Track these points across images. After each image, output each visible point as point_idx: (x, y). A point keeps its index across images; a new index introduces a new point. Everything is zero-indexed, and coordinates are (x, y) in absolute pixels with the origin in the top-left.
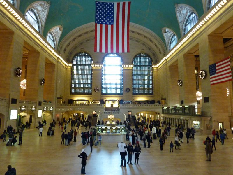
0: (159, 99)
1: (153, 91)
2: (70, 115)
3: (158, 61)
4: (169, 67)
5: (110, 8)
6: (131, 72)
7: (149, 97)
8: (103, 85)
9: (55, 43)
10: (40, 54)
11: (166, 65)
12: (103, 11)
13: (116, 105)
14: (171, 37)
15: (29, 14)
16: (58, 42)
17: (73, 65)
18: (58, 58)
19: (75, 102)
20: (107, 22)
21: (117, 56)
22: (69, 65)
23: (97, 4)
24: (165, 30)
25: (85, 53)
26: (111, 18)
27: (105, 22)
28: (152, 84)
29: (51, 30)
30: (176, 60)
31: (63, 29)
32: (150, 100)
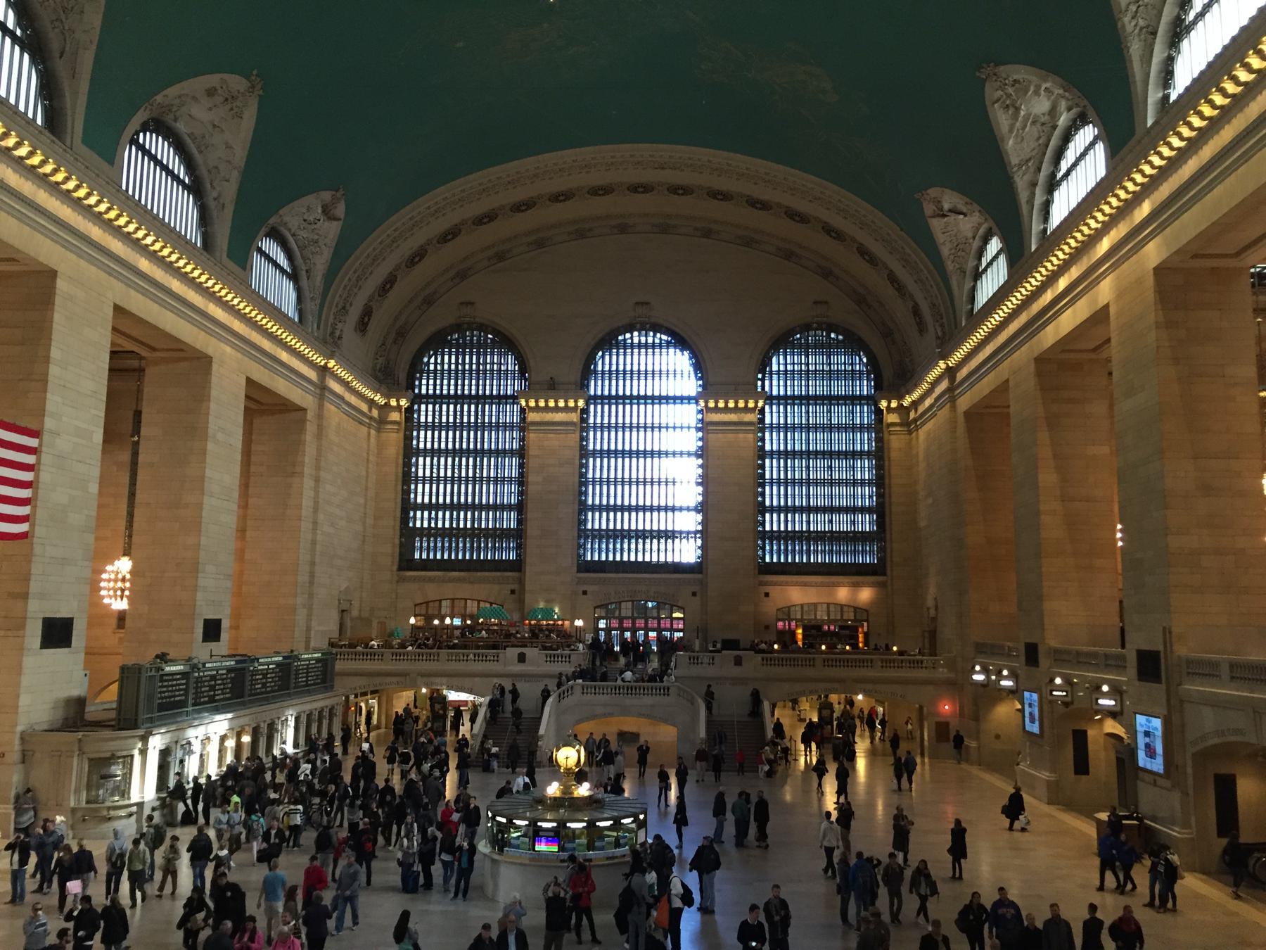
1: (882, 550)
4: (967, 414)
8: (590, 514)
9: (304, 282)
10: (215, 367)
11: (953, 400)
14: (976, 244)
15: (146, 152)
16: (318, 279)
17: (419, 399)
21: (668, 344)
24: (938, 202)
25: (483, 328)
28: (880, 511)
29: (272, 221)
30: (998, 382)
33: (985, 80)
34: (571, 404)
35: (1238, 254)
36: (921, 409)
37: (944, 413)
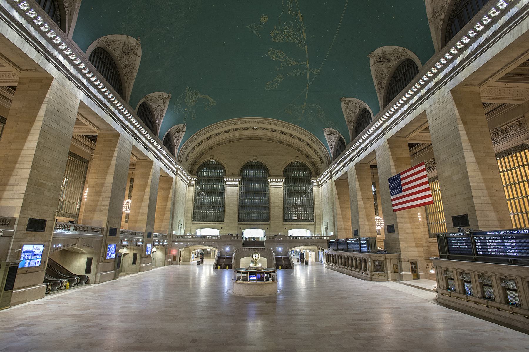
11: (331, 178)
22: (193, 179)
34: (237, 180)
35: (480, 85)
36: (322, 182)
37: (329, 181)
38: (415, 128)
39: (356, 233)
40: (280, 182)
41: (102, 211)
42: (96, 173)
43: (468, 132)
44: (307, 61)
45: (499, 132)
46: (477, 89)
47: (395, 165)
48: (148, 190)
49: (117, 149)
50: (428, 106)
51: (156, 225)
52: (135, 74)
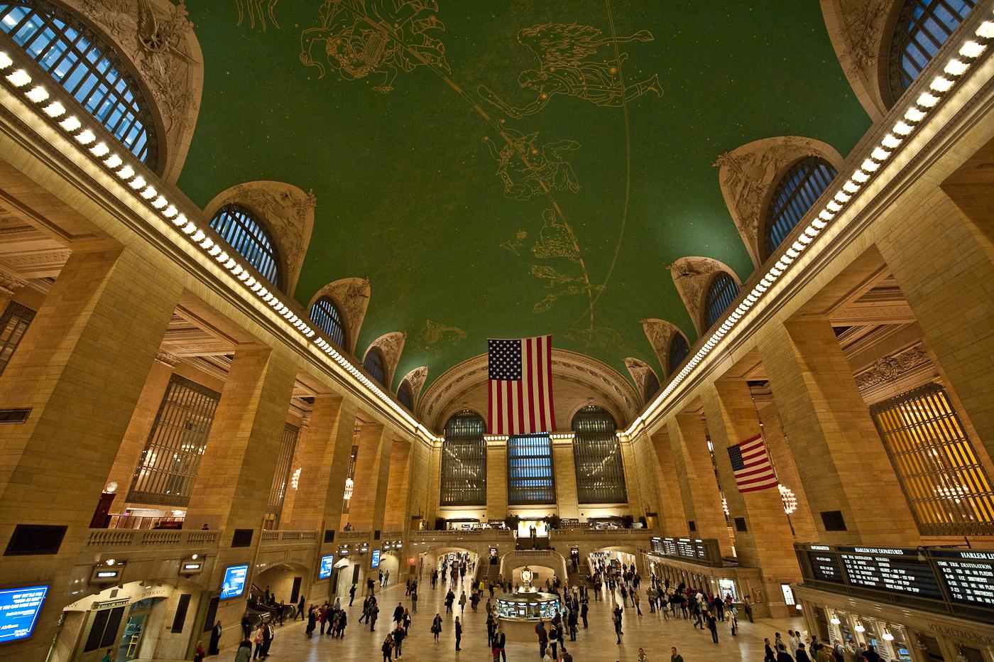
0: (643, 514)
2: (439, 558)
3: (628, 424)
5: (515, 349)
6: (570, 449)
7: (617, 507)
12: (501, 356)
13: (542, 531)
18: (417, 429)
19: (450, 524)
20: (509, 376)
22: (439, 439)
23: (491, 345)
26: (517, 376)
27: (506, 375)
31: (428, 373)
32: (621, 516)
33: (642, 324)
38: (752, 366)
39: (692, 526)
40: (568, 438)
41: (316, 507)
42: (310, 453)
43: (820, 382)
44: (586, 276)
45: (892, 363)
46: (824, 318)
47: (732, 421)
48: (376, 466)
49: (338, 418)
50: (759, 339)
51: (387, 518)
52: (362, 318)
